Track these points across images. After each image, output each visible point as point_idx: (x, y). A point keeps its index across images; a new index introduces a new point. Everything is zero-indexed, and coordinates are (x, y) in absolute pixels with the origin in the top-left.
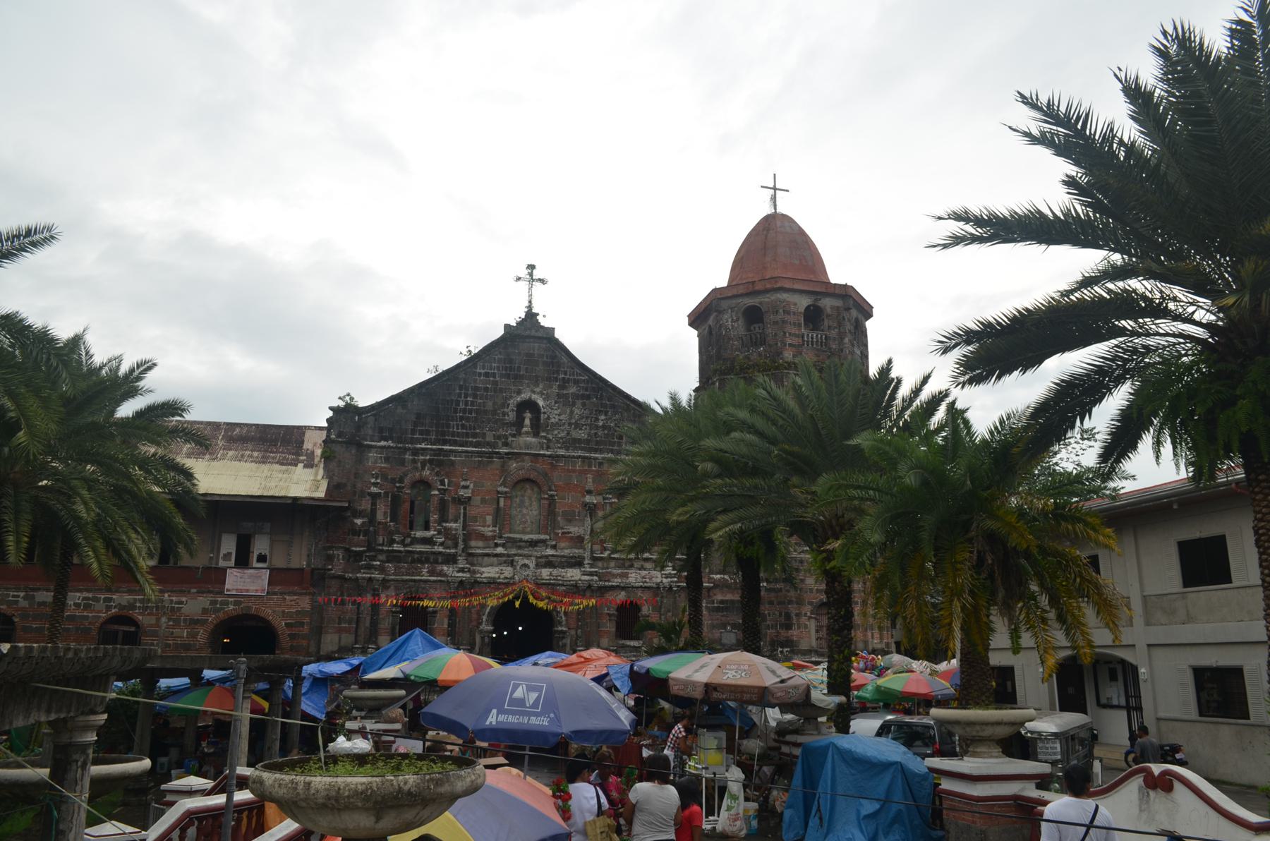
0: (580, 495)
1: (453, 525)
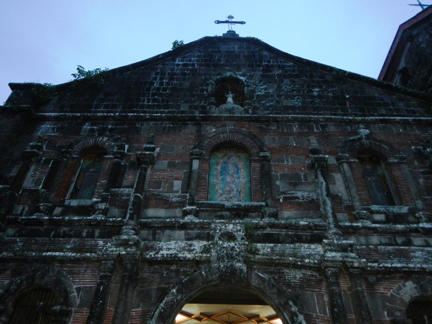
0: (303, 158)
1: (127, 190)
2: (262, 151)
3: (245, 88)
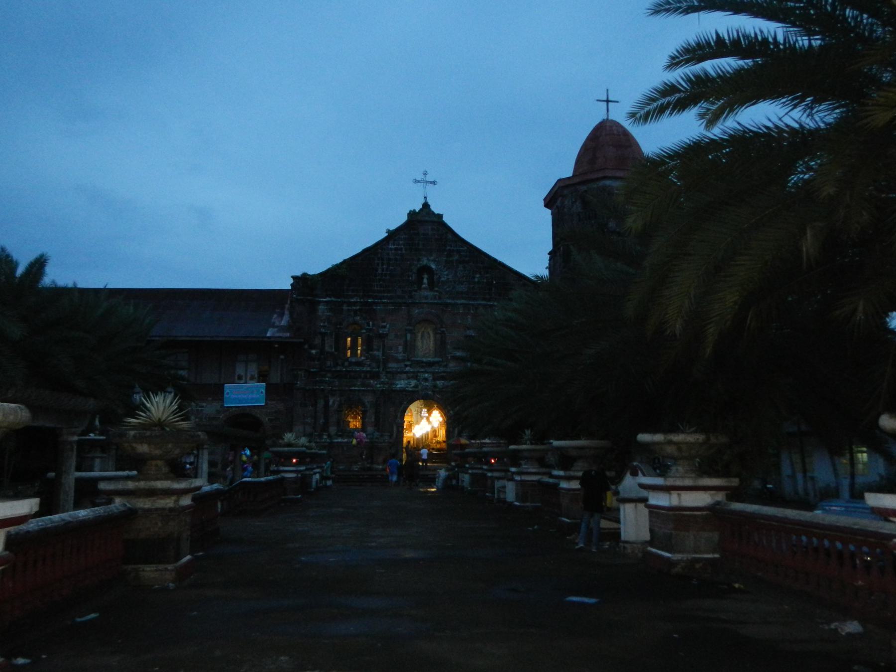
1: (376, 353)
2: (442, 327)
3: (435, 276)
